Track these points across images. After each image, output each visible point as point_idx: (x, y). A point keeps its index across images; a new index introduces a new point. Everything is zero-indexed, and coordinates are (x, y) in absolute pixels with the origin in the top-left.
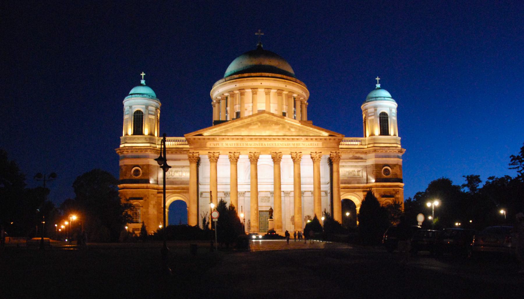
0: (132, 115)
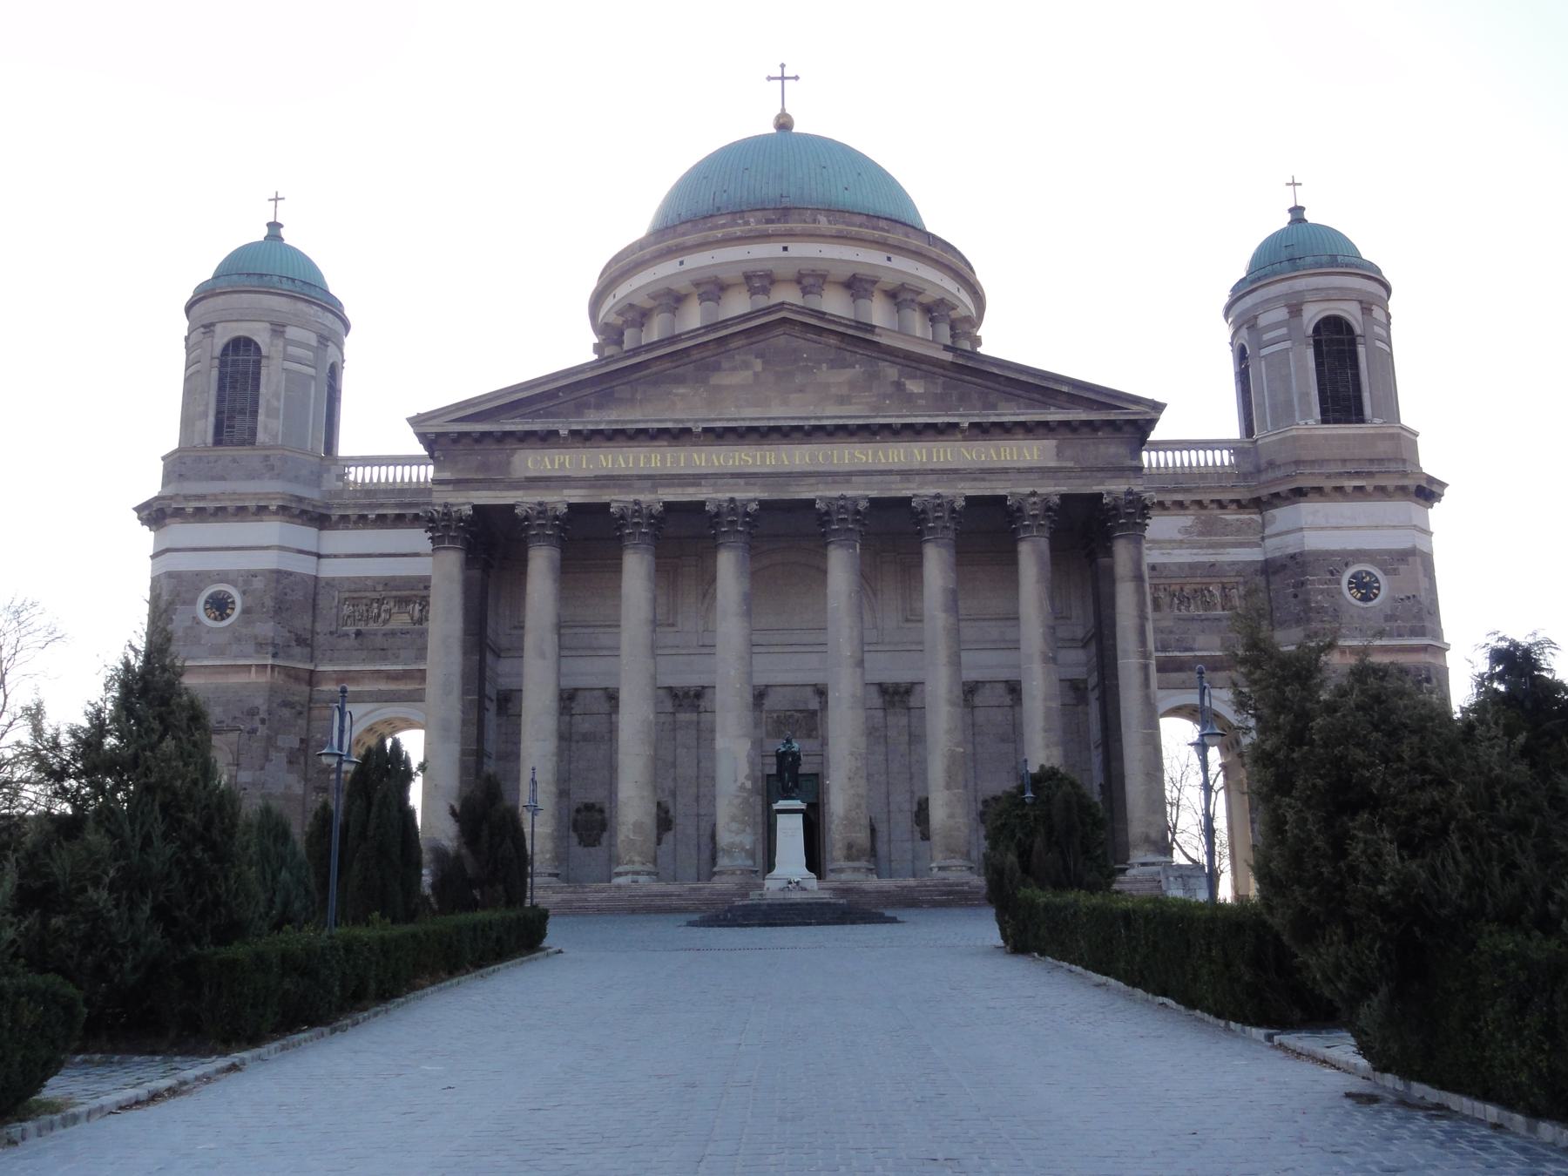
0: (212, 358)
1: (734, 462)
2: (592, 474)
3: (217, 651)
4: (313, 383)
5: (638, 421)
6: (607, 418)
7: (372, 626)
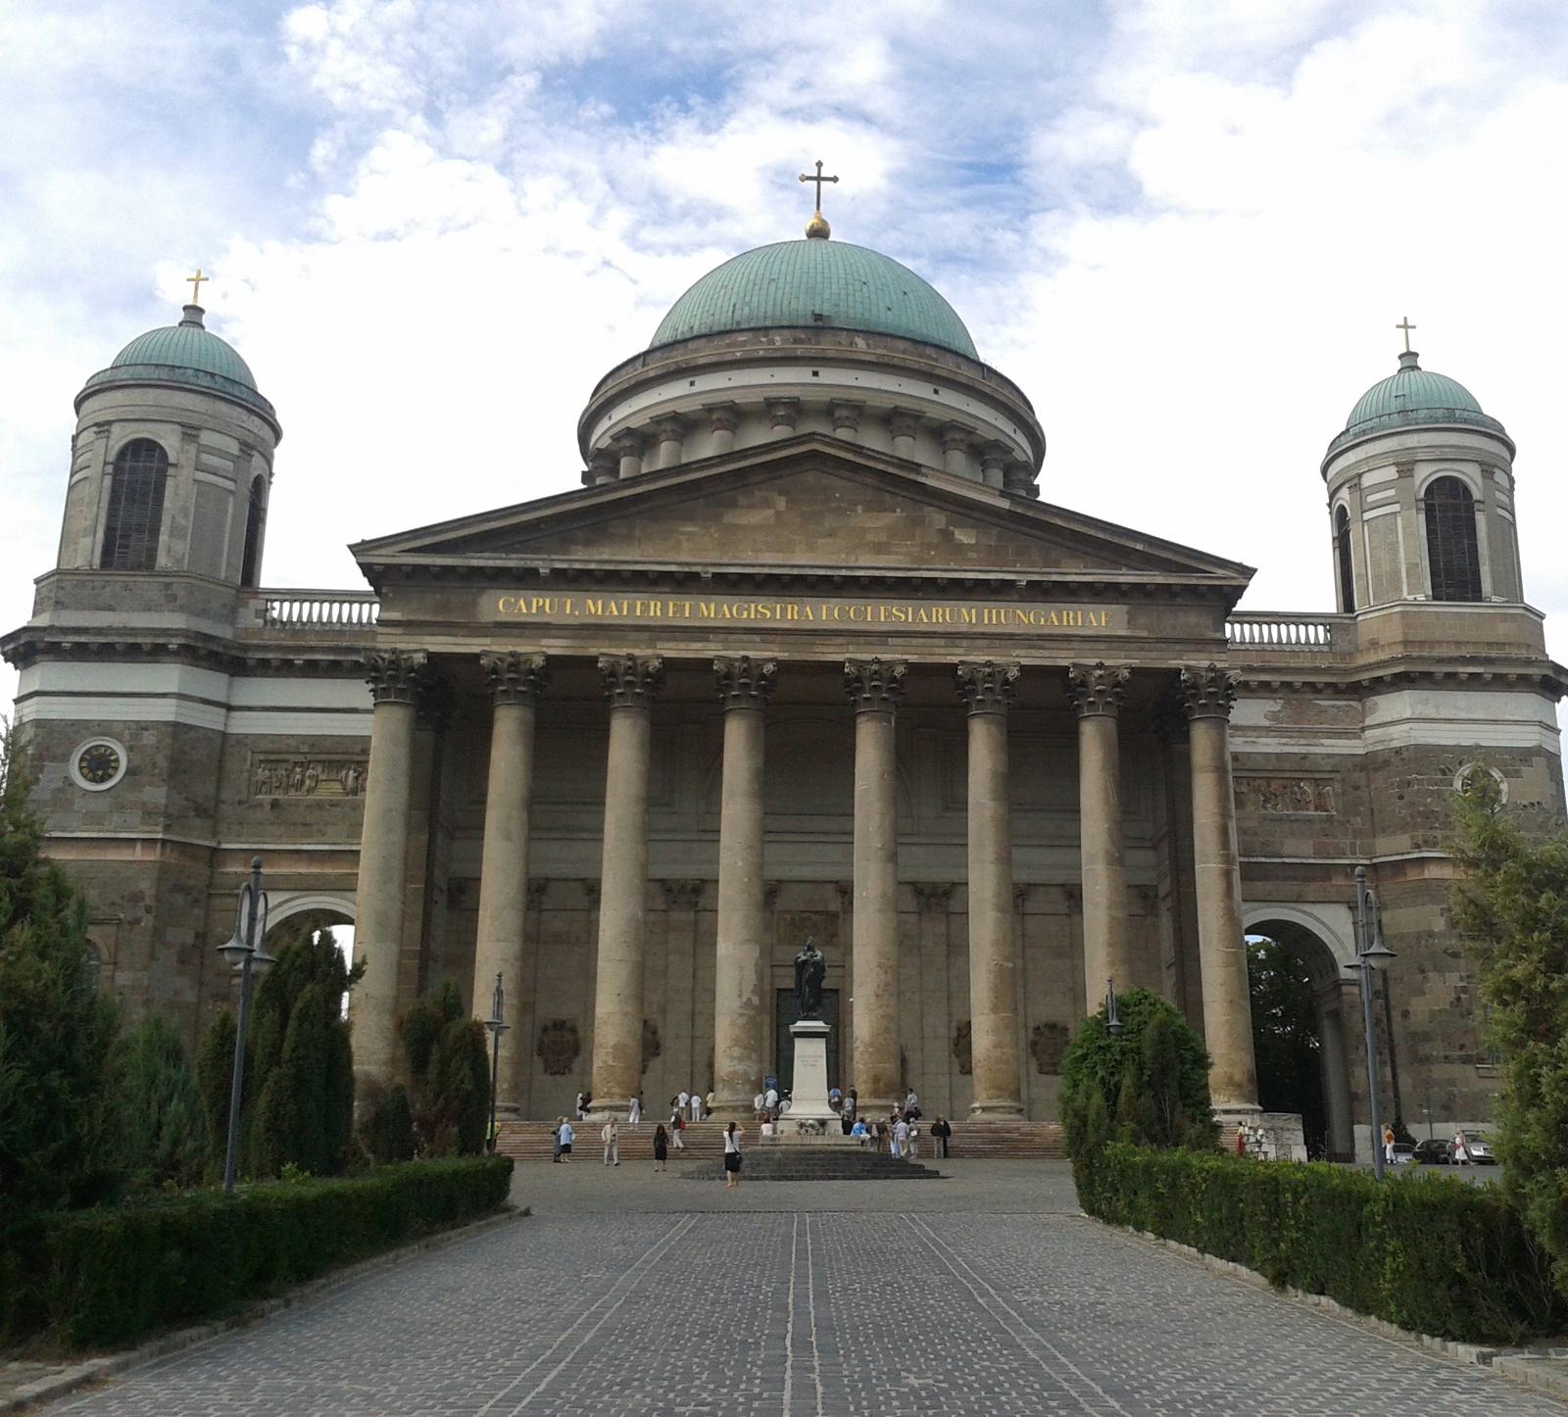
0: (106, 463)
1: (749, 614)
2: (577, 622)
3: (93, 819)
4: (231, 499)
5: (637, 562)
6: (597, 557)
7: (293, 794)
